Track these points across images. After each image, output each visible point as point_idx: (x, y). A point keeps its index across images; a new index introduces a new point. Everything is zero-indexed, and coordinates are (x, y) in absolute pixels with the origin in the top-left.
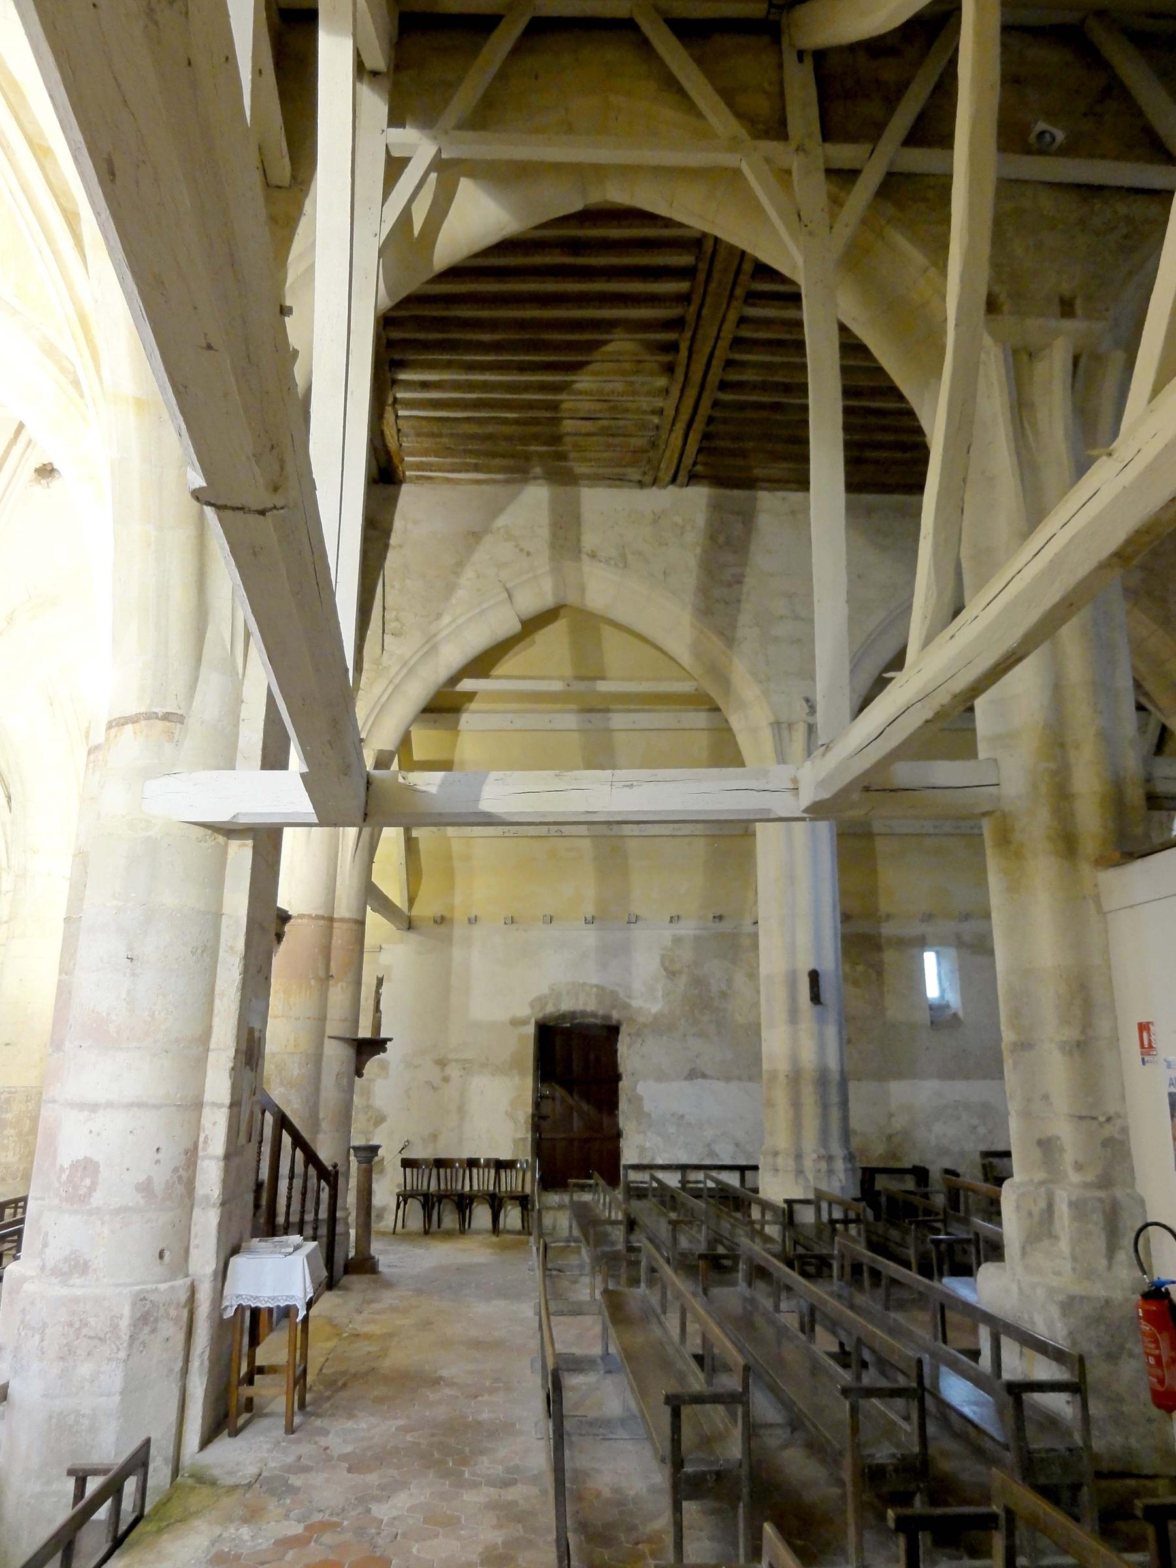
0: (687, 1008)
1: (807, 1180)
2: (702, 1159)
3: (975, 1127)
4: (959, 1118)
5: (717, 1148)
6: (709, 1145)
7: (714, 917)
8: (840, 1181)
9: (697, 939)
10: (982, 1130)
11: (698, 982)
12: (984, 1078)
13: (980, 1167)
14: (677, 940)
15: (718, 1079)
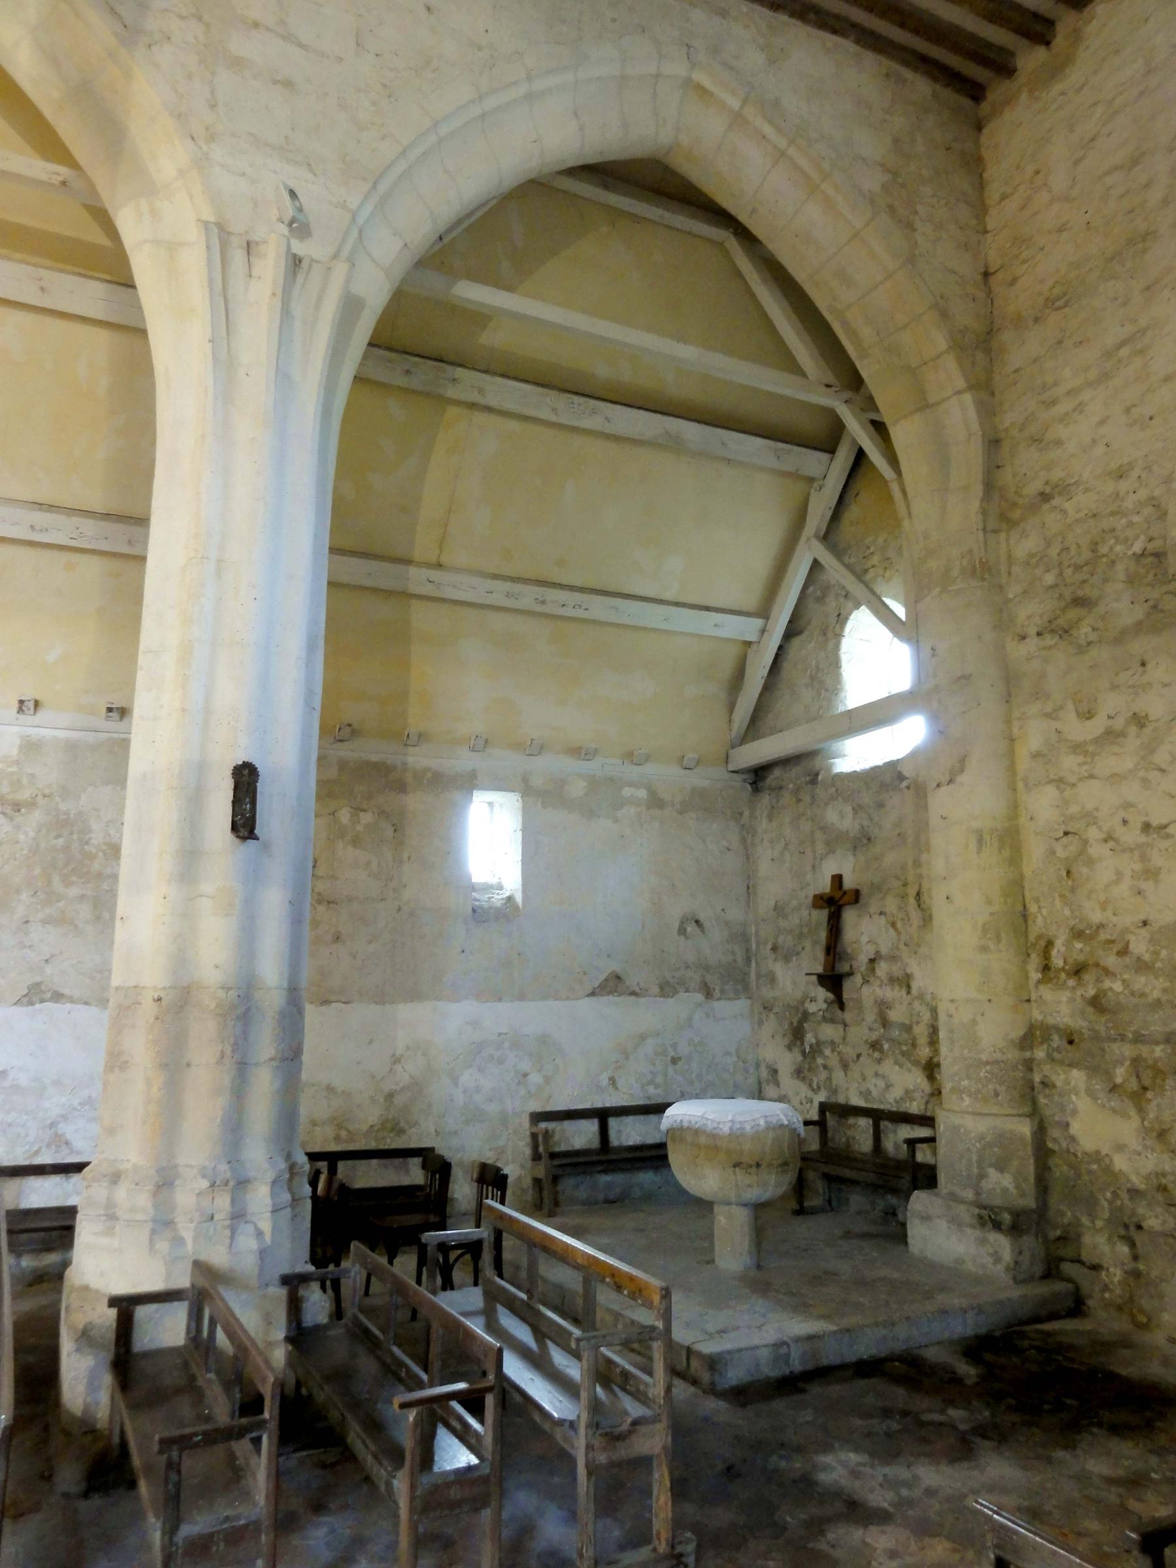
0: (37, 871)
1: (179, 1241)
2: (37, 1153)
3: (525, 1075)
4: (501, 1062)
5: (68, 1130)
6: (53, 1125)
7: (110, 710)
8: (259, 1234)
9: (72, 748)
10: (535, 1078)
11: (62, 824)
12: (545, 998)
13: (528, 1140)
14: (31, 747)
15: (86, 1003)
